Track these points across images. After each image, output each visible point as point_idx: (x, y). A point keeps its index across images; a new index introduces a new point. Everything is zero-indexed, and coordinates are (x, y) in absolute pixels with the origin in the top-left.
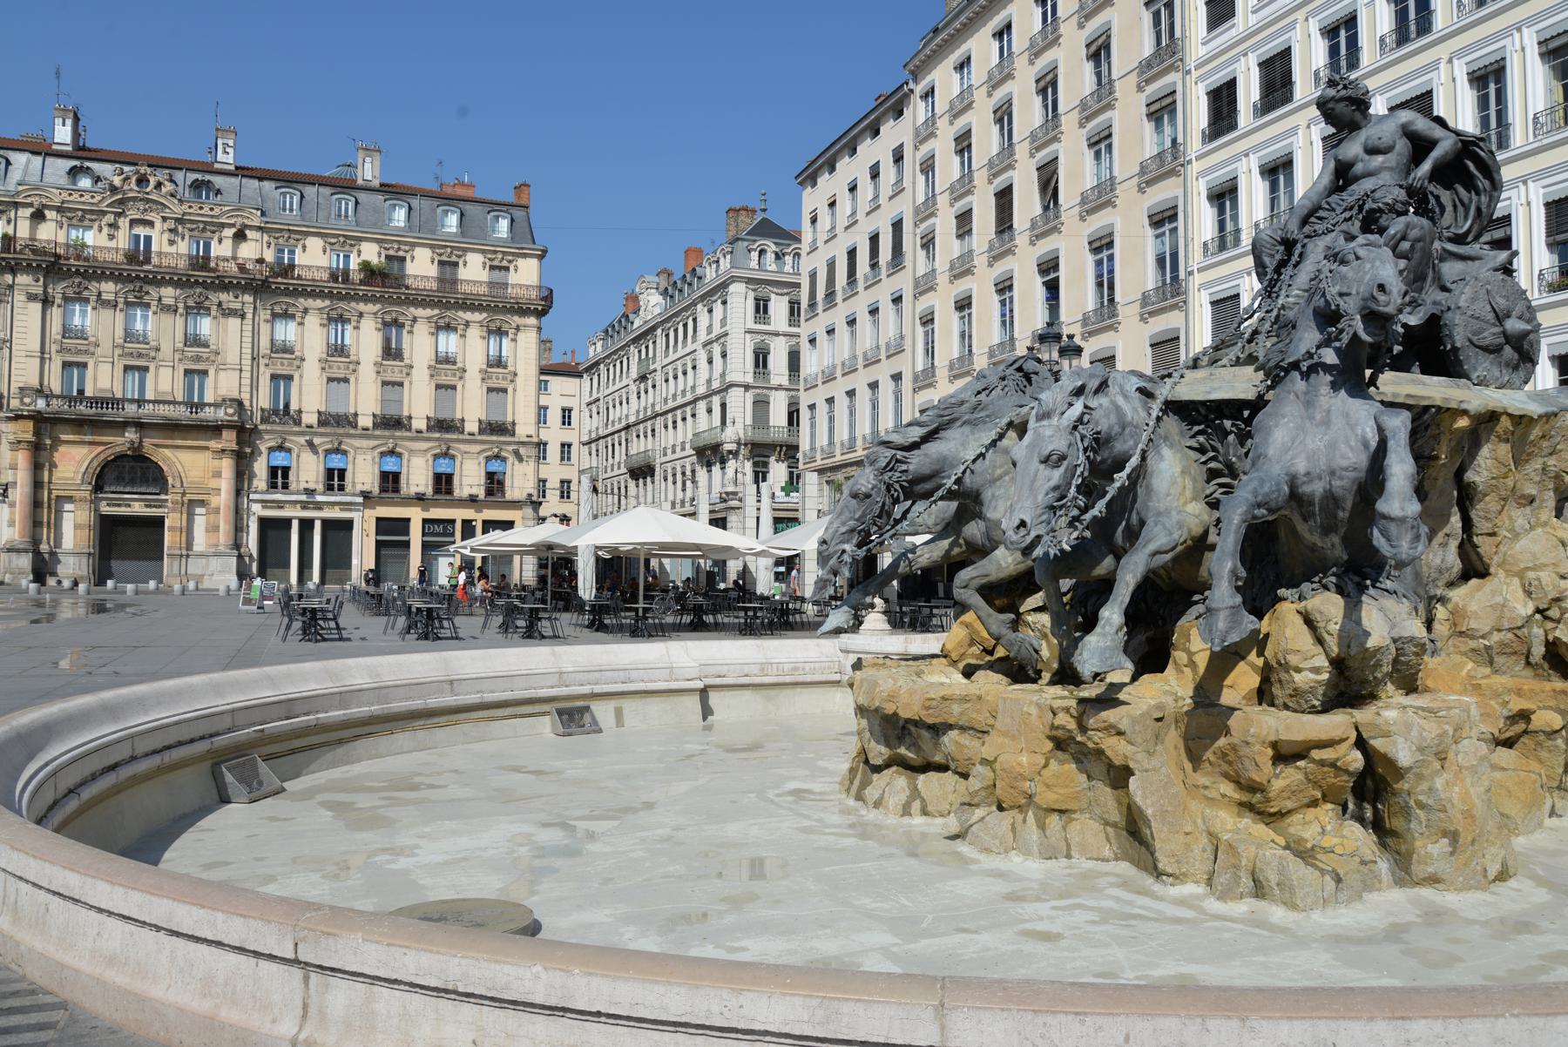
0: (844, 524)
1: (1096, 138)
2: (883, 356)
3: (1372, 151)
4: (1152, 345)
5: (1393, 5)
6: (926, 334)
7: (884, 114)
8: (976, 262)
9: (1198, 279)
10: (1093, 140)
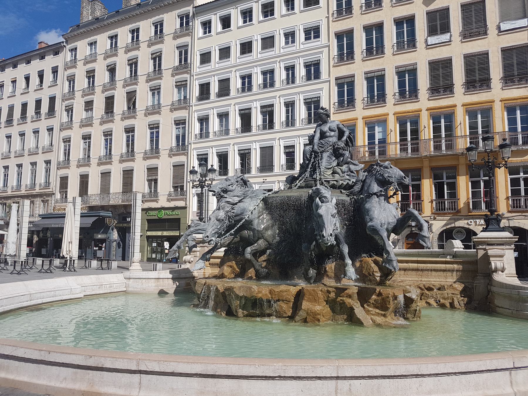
0: (213, 230)
1: (154, 88)
2: (40, 151)
3: (331, 130)
4: (173, 166)
5: (263, 76)
6: (65, 146)
7: (48, 51)
8: (94, 122)
9: (193, 146)
10: (152, 88)
